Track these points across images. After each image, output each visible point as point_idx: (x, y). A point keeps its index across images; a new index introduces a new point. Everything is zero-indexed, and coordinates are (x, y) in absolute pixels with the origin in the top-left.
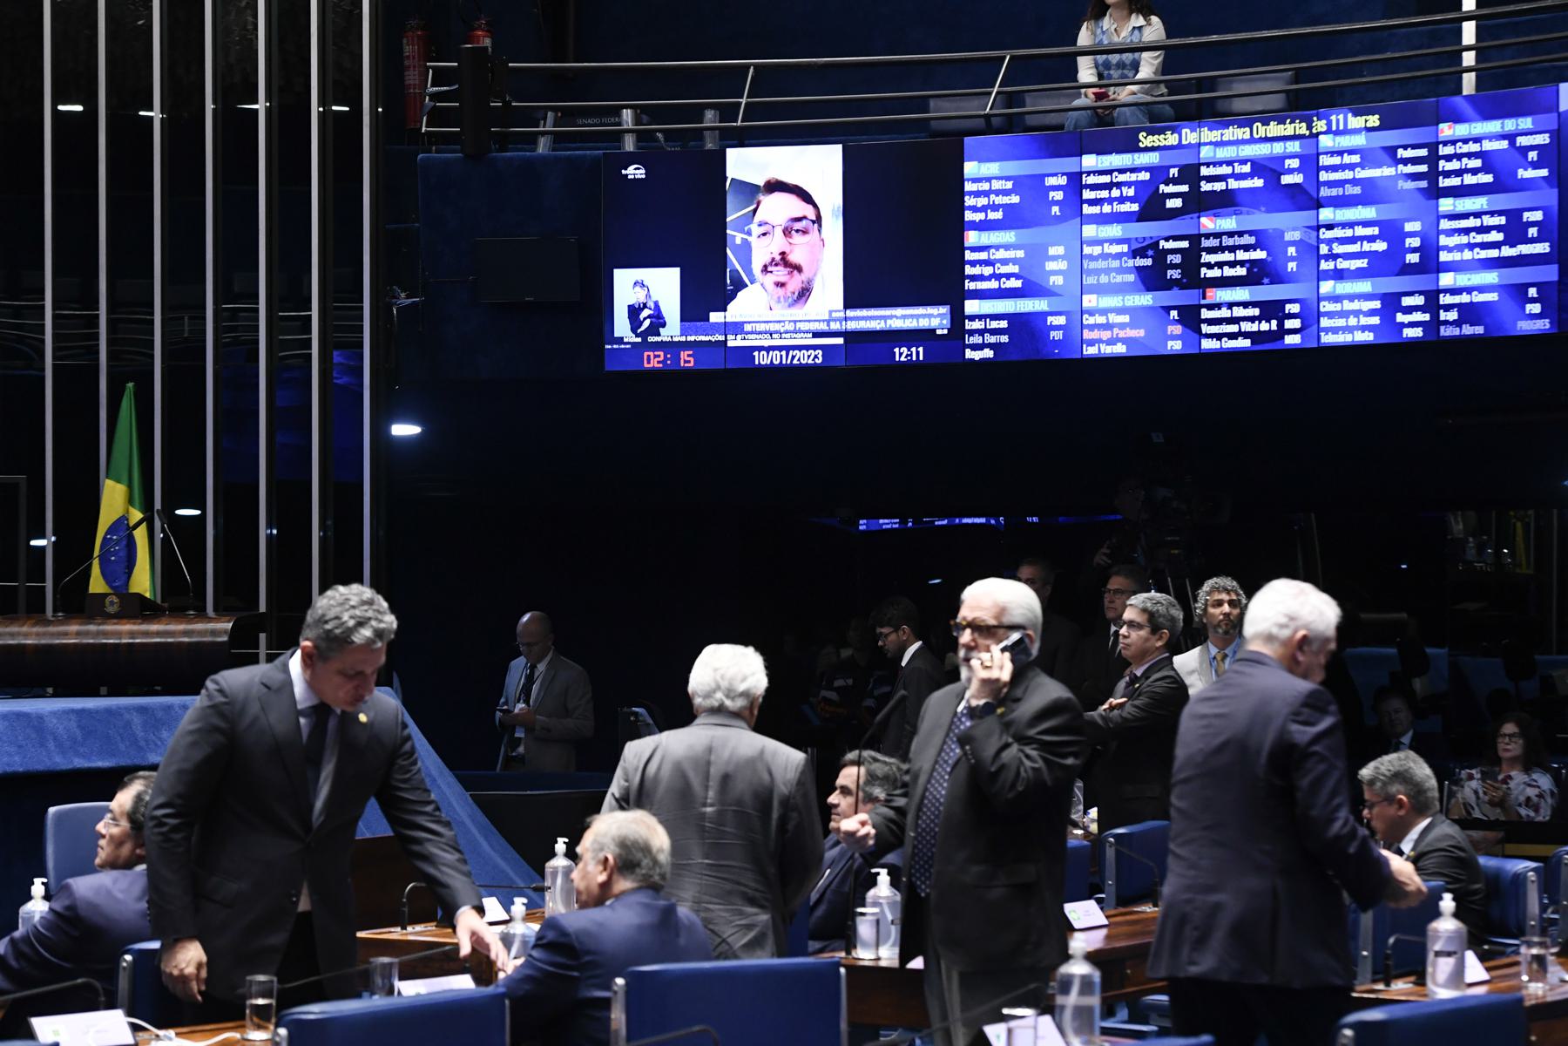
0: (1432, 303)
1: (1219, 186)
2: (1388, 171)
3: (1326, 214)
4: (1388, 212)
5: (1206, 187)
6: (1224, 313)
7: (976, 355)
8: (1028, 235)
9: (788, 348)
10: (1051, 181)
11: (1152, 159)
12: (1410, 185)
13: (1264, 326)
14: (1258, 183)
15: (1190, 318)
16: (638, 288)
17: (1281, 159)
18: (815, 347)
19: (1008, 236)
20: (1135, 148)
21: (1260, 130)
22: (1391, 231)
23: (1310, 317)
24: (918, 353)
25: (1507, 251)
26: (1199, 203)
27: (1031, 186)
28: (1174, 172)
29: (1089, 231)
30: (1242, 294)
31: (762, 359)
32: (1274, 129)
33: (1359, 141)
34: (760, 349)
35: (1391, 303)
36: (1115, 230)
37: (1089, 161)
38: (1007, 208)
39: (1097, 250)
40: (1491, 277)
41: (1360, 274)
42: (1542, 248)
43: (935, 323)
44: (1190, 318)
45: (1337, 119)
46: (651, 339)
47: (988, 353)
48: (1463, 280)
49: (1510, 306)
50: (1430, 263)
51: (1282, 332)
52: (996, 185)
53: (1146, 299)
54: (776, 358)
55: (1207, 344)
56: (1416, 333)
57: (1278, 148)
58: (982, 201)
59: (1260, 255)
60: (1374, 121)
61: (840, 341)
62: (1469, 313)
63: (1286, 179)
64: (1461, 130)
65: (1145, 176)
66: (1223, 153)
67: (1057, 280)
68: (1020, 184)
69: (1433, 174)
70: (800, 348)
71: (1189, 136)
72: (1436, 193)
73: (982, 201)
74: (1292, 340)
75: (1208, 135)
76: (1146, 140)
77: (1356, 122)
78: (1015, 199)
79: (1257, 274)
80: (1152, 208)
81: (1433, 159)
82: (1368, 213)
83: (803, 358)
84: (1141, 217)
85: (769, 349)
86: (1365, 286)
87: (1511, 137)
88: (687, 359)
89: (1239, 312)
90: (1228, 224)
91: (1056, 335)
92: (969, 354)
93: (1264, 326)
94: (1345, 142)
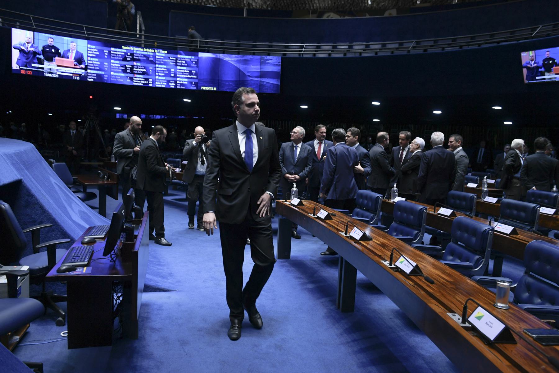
0: (176, 82)
1: (137, 58)
2: (169, 61)
3: (157, 66)
4: (169, 67)
5: (135, 57)
6: (138, 79)
7: (90, 80)
8: (101, 60)
10: (105, 51)
11: (125, 51)
12: (172, 63)
13: (145, 82)
14: (145, 58)
15: (131, 79)
17: (149, 55)
19: (97, 60)
20: (121, 48)
21: (145, 50)
22: (169, 70)
23: (154, 82)
24: (78, 78)
25: (189, 76)
26: (133, 60)
27: (101, 52)
28: (129, 54)
29: (112, 61)
30: (141, 76)
32: (148, 50)
33: (164, 55)
35: (168, 82)
36: (118, 62)
37: (112, 49)
38: (96, 55)
39: (114, 65)
40: (186, 80)
41: (163, 76)
42: (195, 77)
44: (131, 79)
45: (160, 51)
47: (92, 80)
48: (181, 79)
49: (190, 85)
50: (175, 76)
51: (148, 83)
52: (94, 50)
53: (123, 75)
55: (134, 84)
56: (173, 87)
57: (149, 53)
58: (91, 52)
59: (145, 70)
60: (166, 52)
62: (182, 85)
63: (150, 59)
64: (182, 56)
65: (123, 54)
66: (138, 52)
67: (106, 69)
68: (99, 51)
69: (176, 63)
71: (132, 48)
72: (177, 65)
73: (91, 52)
74: (150, 85)
75: (135, 49)
76: (123, 47)
77: (163, 52)
78: (98, 53)
79: (144, 73)
80: (125, 59)
81: (176, 60)
82: (165, 67)
84: (123, 60)
86: (164, 78)
87: (190, 59)
89: (141, 79)
90: (139, 64)
91: (105, 78)
92: (88, 80)
93: (145, 82)
94: (161, 55)
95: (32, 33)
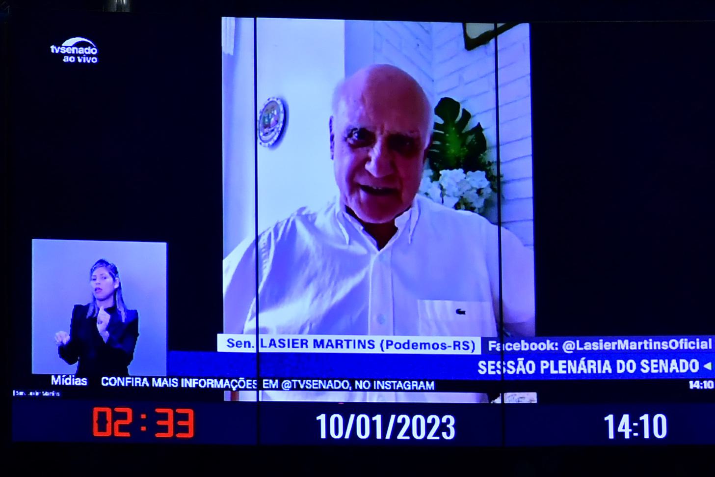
9: (387, 410)
16: (103, 271)
18: (440, 409)
24: (657, 426)
31: (331, 428)
34: (330, 408)
43: (691, 366)
46: (108, 381)
54: (362, 427)
61: (530, 397)
70: (411, 409)
83: (417, 428)
85: (347, 409)
88: (177, 426)
95: (458, 26)
